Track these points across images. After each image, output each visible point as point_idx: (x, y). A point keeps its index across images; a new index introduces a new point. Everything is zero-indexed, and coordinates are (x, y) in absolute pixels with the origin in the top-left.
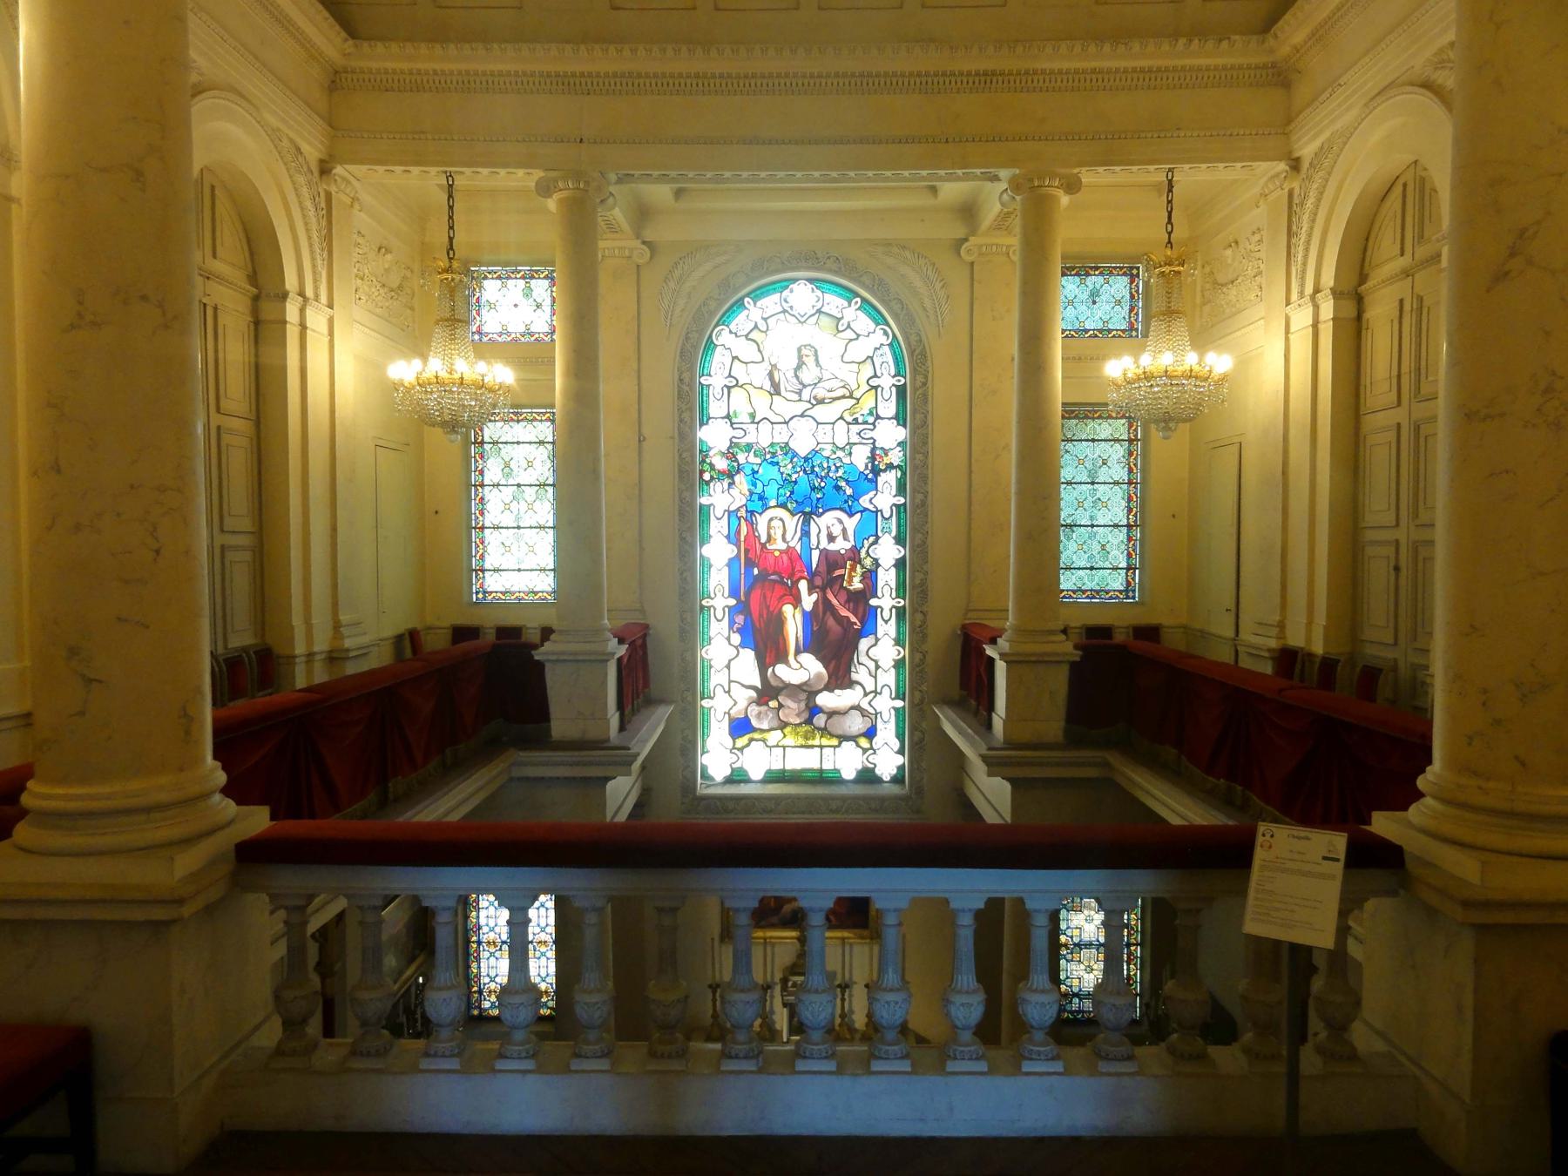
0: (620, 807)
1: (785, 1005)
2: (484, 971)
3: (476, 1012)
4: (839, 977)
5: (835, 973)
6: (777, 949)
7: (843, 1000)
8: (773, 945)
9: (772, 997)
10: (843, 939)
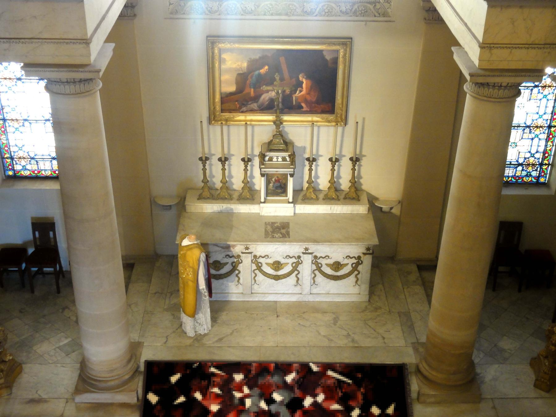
0: (103, 18)
1: (262, 175)
2: (12, 143)
3: (11, 173)
4: (308, 150)
5: (304, 148)
6: (257, 129)
7: (310, 170)
8: (253, 126)
9: (252, 166)
10: (313, 123)
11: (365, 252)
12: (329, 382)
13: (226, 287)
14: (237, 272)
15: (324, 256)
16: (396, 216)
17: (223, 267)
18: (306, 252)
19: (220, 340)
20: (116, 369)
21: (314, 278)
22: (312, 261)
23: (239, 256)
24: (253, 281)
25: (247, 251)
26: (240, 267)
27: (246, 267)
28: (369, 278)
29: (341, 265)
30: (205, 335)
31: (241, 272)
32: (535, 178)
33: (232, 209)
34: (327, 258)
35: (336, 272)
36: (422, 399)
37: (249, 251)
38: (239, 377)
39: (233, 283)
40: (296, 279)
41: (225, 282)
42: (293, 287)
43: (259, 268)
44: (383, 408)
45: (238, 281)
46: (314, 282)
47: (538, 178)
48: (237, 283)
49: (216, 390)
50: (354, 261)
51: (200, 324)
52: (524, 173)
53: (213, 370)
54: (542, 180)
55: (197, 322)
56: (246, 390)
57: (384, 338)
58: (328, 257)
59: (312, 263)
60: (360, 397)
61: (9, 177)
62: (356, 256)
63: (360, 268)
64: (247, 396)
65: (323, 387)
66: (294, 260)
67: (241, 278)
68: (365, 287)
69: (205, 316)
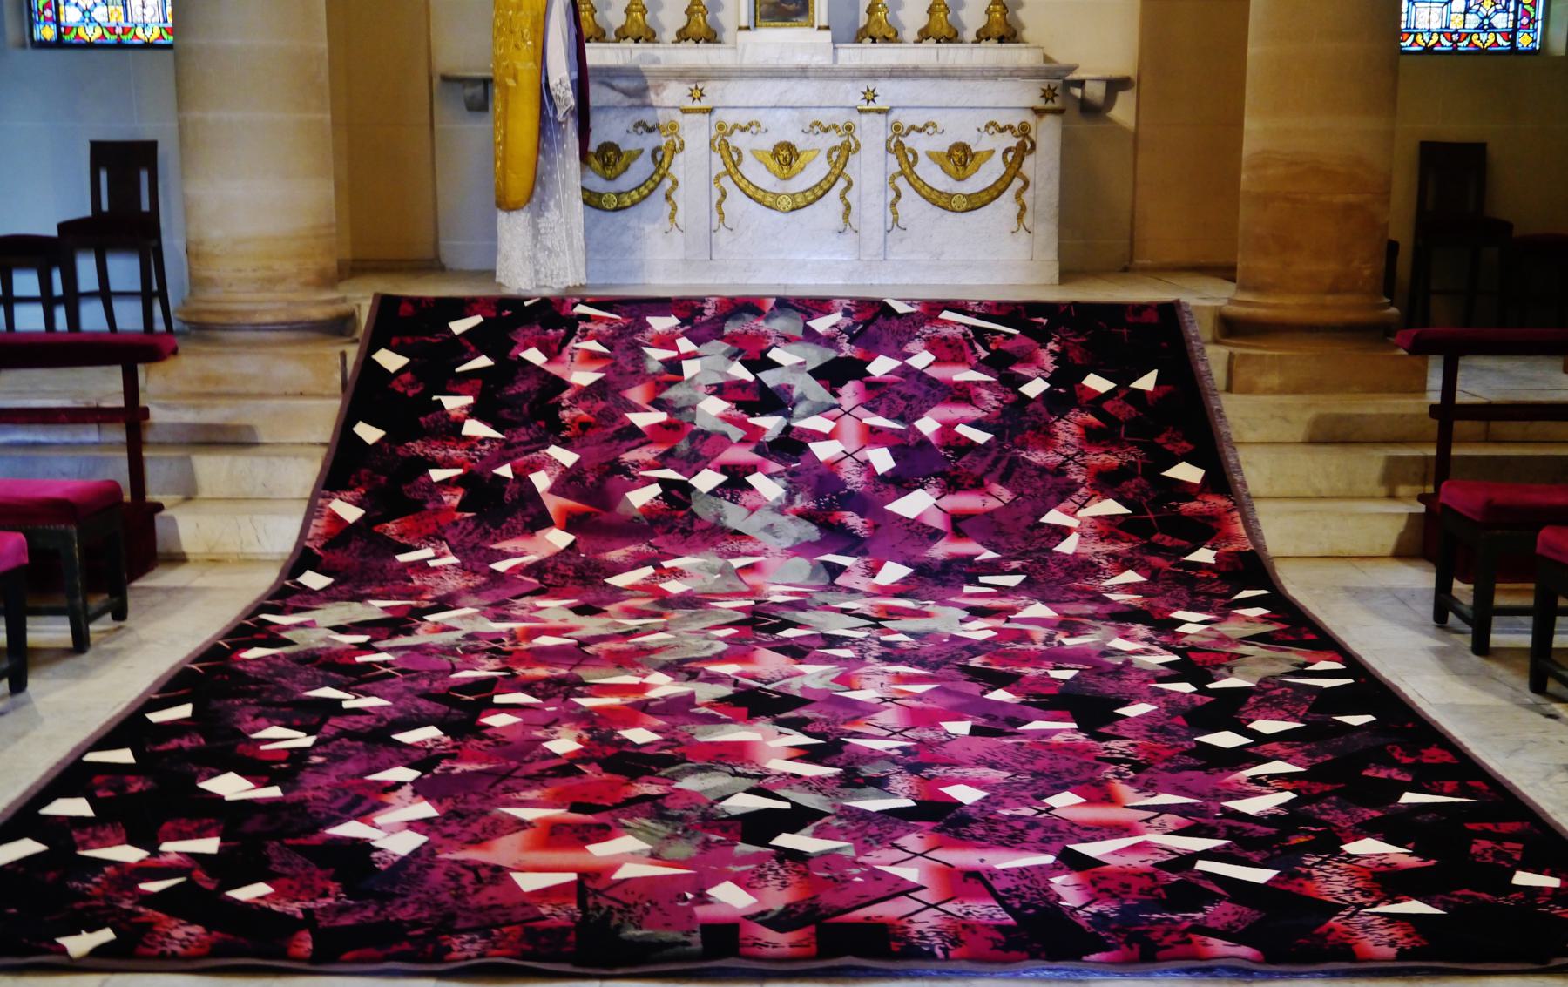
3: (48, 32)
11: (1040, 103)
12: (946, 331)
13: (636, 238)
14: (667, 183)
16: (1123, 129)
17: (626, 168)
18: (870, 107)
20: (283, 279)
21: (893, 204)
22: (888, 142)
23: (674, 126)
24: (716, 216)
25: (697, 105)
26: (679, 167)
27: (693, 167)
28: (1055, 200)
29: (973, 156)
31: (681, 183)
32: (1504, 35)
33: (657, 61)
34: (930, 130)
35: (959, 181)
36: (1242, 375)
37: (704, 104)
38: (661, 324)
41: (633, 223)
43: (733, 162)
44: (1123, 375)
45: (672, 216)
46: (895, 220)
47: (1512, 35)
48: (668, 226)
49: (593, 346)
50: (1013, 142)
51: (550, 251)
52: (1473, 21)
53: (581, 309)
54: (1524, 41)
56: (685, 345)
58: (934, 125)
59: (888, 149)
60: (1048, 361)
61: (44, 44)
62: (1016, 125)
63: (1028, 165)
64: (690, 356)
65: (927, 340)
66: (834, 139)
67: (680, 207)
68: (1046, 232)
69: (566, 214)
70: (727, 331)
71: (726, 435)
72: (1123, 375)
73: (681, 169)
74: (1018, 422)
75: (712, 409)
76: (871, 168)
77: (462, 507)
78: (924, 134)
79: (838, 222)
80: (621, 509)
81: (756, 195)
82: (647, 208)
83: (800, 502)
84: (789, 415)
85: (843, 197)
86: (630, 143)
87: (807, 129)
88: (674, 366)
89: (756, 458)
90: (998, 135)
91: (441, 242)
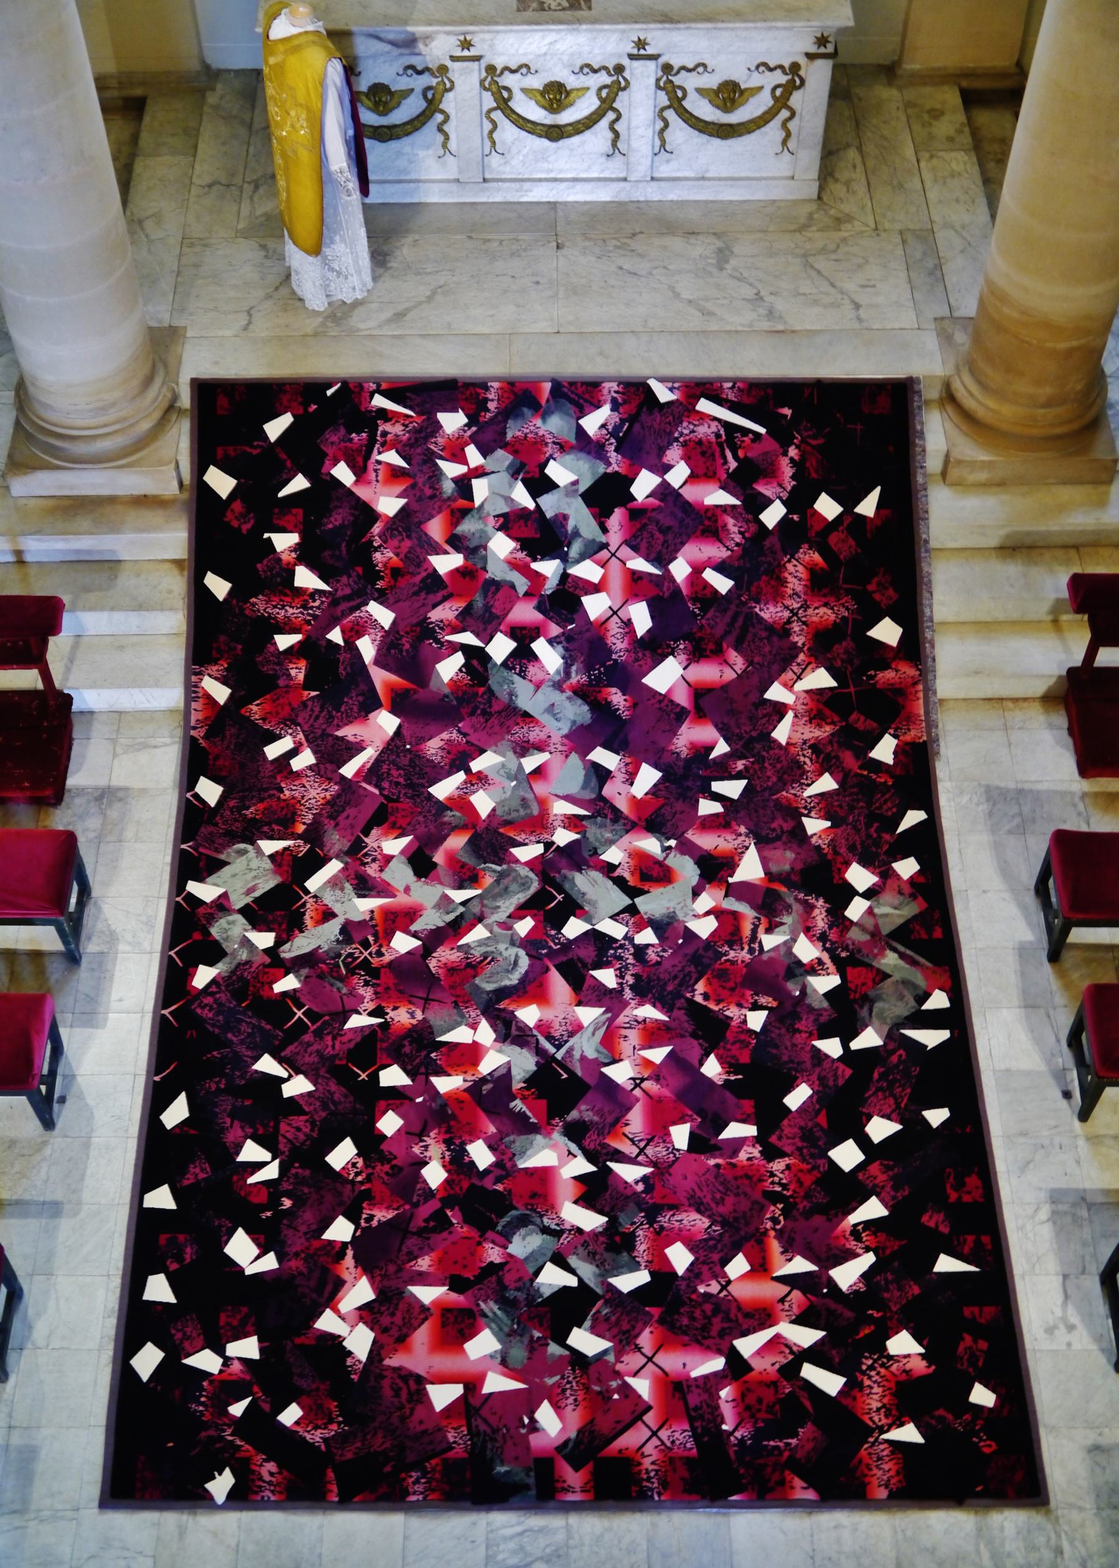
11: (813, 49)
12: (704, 431)
13: (411, 162)
14: (439, 117)
15: (691, 66)
17: (398, 105)
19: (399, 316)
20: (113, 405)
22: (658, 80)
23: (443, 69)
24: (488, 144)
25: (466, 53)
26: (449, 103)
27: (466, 98)
29: (742, 92)
30: (357, 304)
34: (701, 69)
36: (954, 473)
37: (473, 52)
38: (452, 422)
39: (430, 152)
40: (610, 135)
42: (604, 159)
43: (503, 103)
44: (849, 499)
45: (445, 146)
48: (441, 152)
49: (392, 457)
50: (783, 79)
51: (339, 273)
53: (379, 401)
55: (332, 270)
57: (857, 306)
58: (704, 66)
59: (658, 87)
62: (787, 65)
63: (796, 99)
64: (479, 472)
65: (685, 445)
66: (604, 79)
67: (453, 136)
69: (351, 247)
70: (509, 436)
71: (512, 586)
72: (849, 499)
73: (452, 104)
74: (756, 562)
75: (501, 546)
76: (641, 101)
77: (308, 684)
78: (694, 73)
79: (607, 146)
80: (433, 685)
81: (522, 123)
82: (419, 137)
83: (576, 678)
84: (564, 558)
85: (612, 128)
86: (399, 84)
87: (577, 70)
88: (464, 485)
89: (538, 616)
90: (767, 73)
91: (205, 44)
